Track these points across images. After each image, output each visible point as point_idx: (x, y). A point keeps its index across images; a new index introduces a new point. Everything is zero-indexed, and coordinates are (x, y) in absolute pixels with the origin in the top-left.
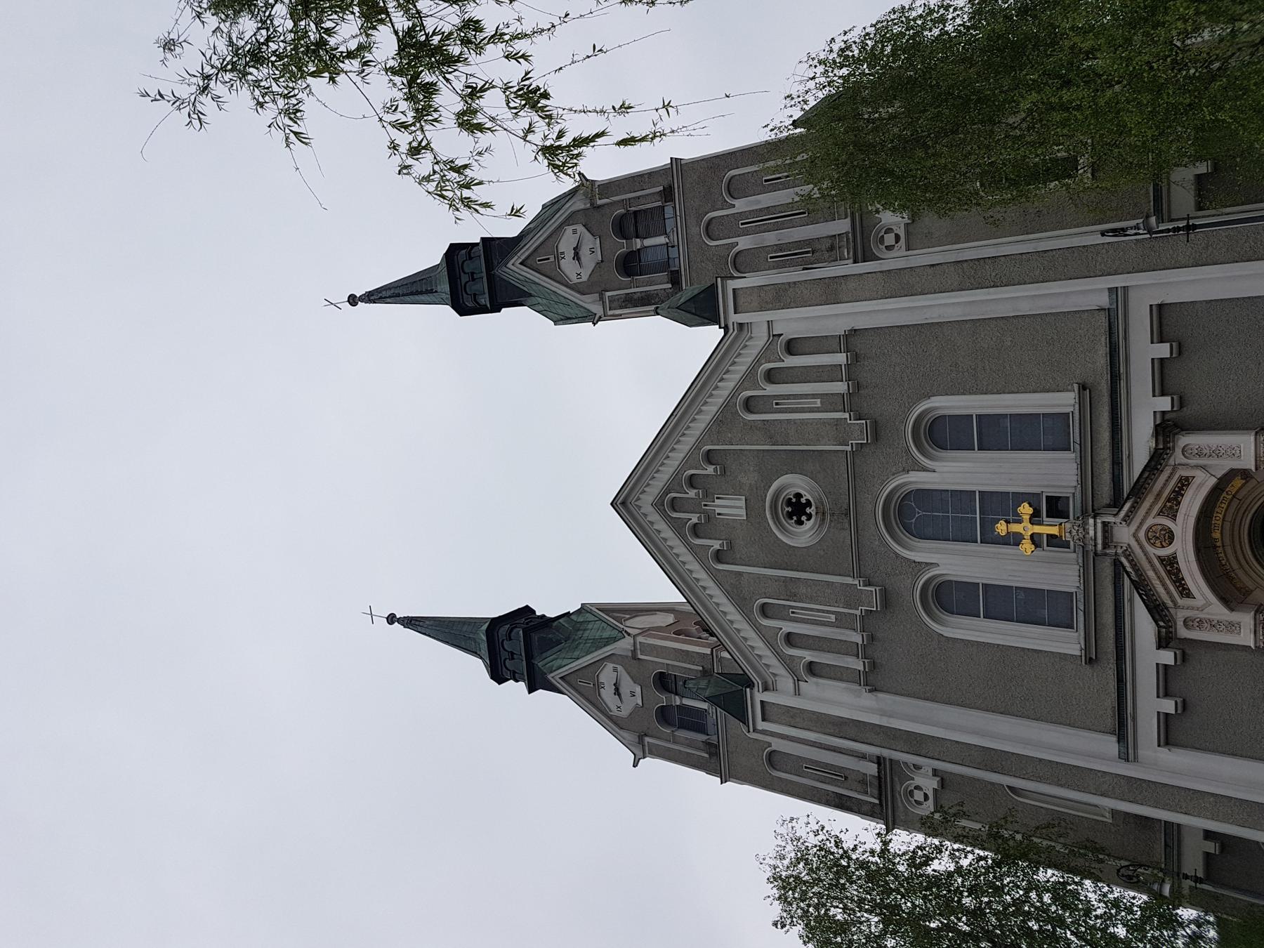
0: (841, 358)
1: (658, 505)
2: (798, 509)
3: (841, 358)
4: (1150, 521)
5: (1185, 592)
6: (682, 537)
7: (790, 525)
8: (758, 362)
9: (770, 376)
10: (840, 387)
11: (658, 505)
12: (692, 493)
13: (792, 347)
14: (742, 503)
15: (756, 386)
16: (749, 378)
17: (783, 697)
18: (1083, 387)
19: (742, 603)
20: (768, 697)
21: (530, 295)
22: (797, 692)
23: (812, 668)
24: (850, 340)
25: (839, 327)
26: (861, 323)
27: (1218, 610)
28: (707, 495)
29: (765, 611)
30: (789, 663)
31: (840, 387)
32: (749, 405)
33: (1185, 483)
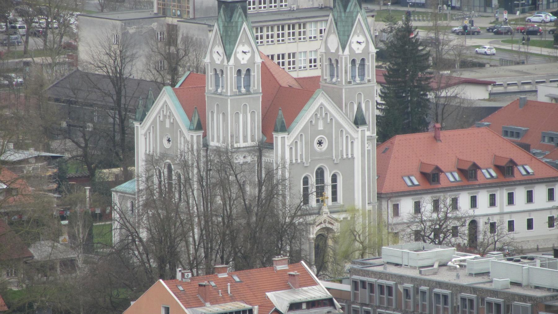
0: (350, 156)
1: (322, 104)
2: (320, 143)
3: (350, 156)
4: (327, 220)
5: (317, 226)
6: (315, 112)
7: (318, 142)
8: (350, 135)
9: (347, 137)
10: (345, 156)
11: (322, 104)
12: (324, 115)
13: (352, 142)
14: (322, 129)
15: (346, 134)
16: (347, 132)
17: (287, 143)
18: (343, 205)
19: (302, 130)
20: (286, 138)
21: (345, 11)
22: (288, 145)
23: (291, 148)
24: (353, 158)
25: (355, 156)
26: (356, 161)
27: (315, 232)
28: (323, 119)
29: (301, 135)
30: (292, 144)
31: (345, 156)
32: (342, 131)
33: (332, 224)
